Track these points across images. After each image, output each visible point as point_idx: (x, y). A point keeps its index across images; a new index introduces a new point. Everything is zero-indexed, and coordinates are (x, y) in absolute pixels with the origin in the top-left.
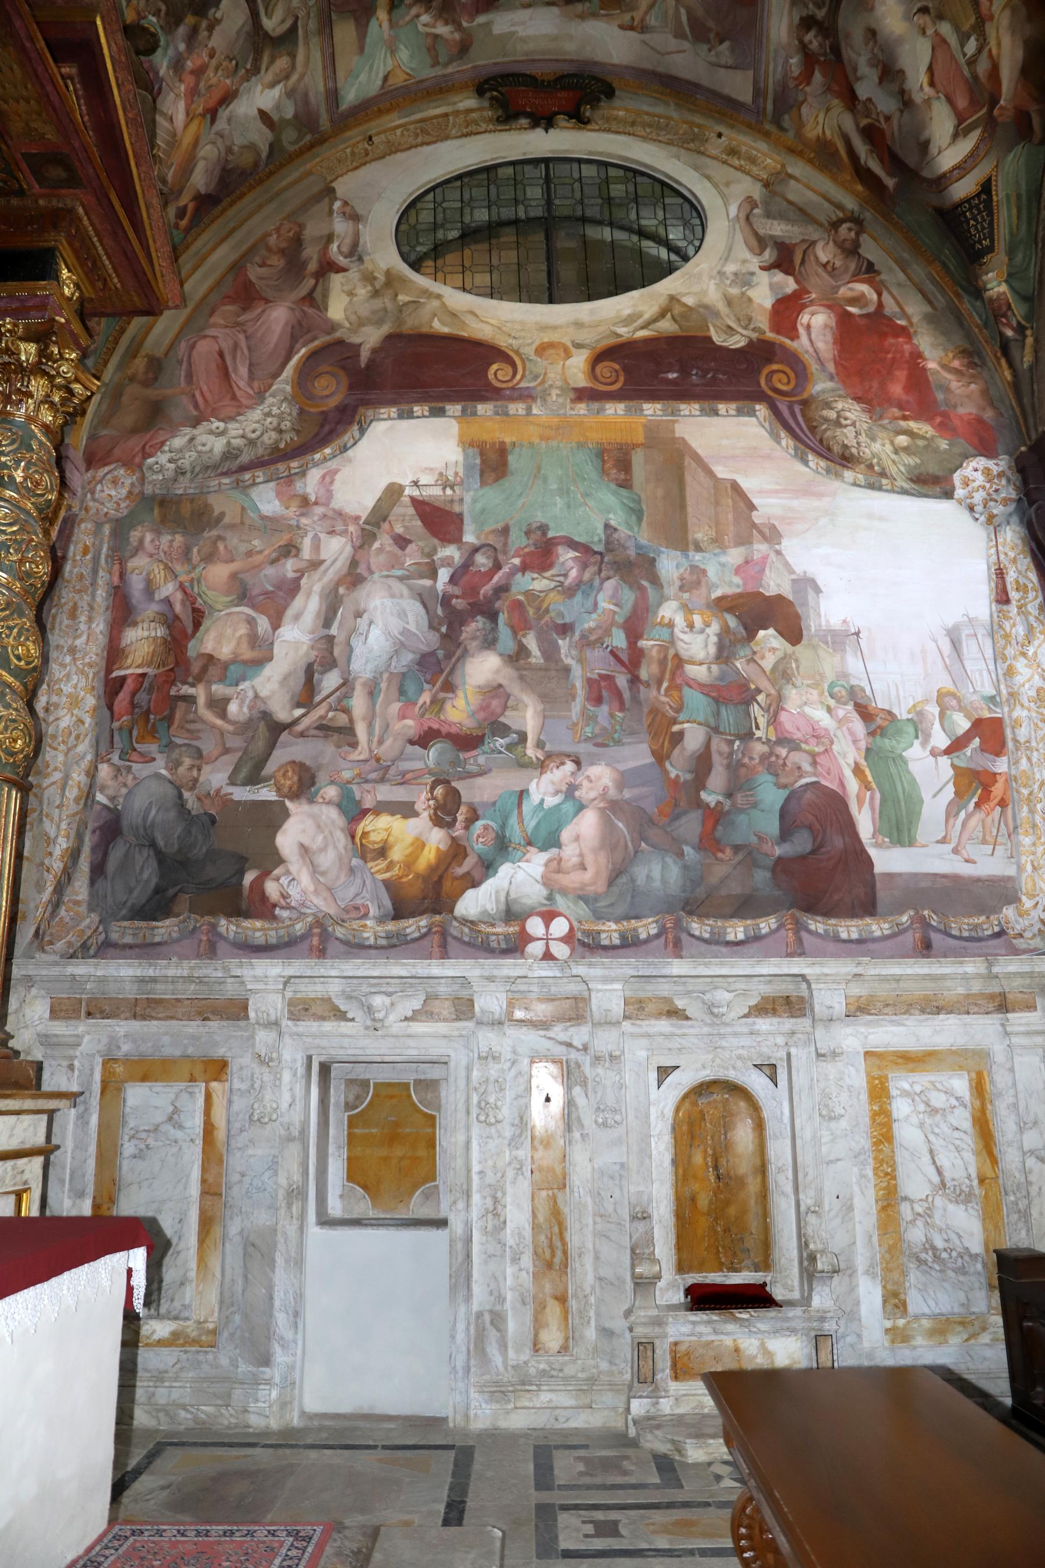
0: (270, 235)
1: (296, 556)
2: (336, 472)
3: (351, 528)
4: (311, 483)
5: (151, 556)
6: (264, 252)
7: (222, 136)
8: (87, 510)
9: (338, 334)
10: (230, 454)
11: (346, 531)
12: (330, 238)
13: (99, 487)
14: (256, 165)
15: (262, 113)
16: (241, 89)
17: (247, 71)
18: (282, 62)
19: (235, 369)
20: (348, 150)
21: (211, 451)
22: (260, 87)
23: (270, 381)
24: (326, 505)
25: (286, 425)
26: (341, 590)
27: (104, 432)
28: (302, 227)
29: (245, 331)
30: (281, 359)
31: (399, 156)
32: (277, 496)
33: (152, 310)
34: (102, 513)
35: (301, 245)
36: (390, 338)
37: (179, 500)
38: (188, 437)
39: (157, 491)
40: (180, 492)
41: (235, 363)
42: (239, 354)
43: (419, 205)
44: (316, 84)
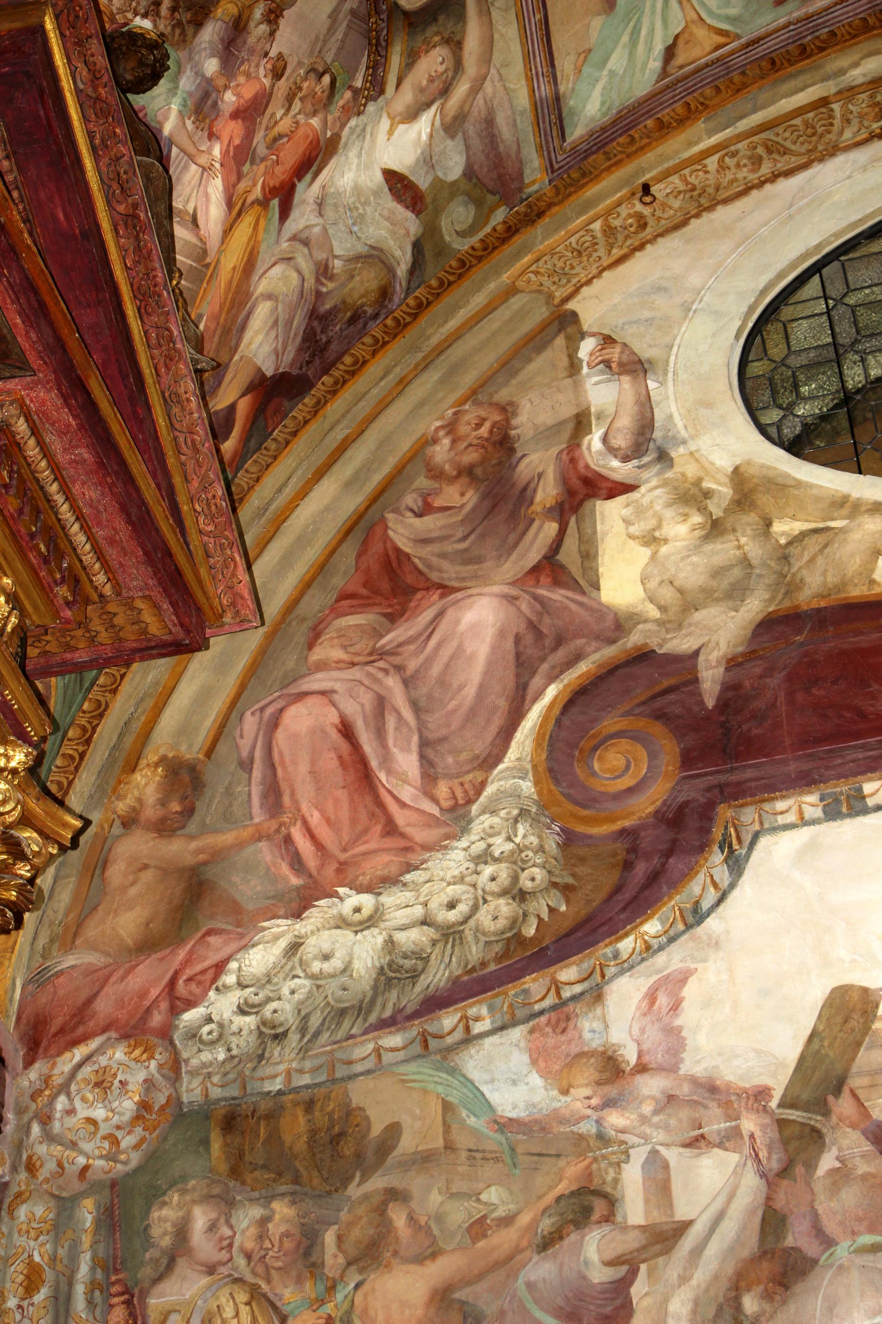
0: (435, 441)
1: (608, 1218)
2: (682, 978)
3: (749, 1124)
4: (620, 1018)
5: (211, 1269)
6: (423, 482)
7: (306, 243)
8: (31, 1168)
9: (634, 639)
10: (395, 971)
11: (737, 1132)
12: (581, 423)
13: (61, 1103)
14: (385, 293)
15: (393, 178)
17: (356, 92)
18: (433, 62)
19: (386, 759)
20: (597, 226)
21: (346, 969)
22: (385, 123)
23: (479, 776)
24: (671, 1069)
25: (534, 876)
26: (750, 1304)
27: (70, 961)
28: (508, 410)
29: (399, 668)
30: (497, 722)
31: (722, 214)
32: (534, 1062)
33: (185, 644)
34: (71, 1171)
35: (512, 450)
36: (768, 625)
37: (273, 1111)
38: (283, 943)
39: (216, 1093)
40: (277, 1085)
41: (384, 745)
42: (391, 722)
43: (787, 312)
44: (510, 91)
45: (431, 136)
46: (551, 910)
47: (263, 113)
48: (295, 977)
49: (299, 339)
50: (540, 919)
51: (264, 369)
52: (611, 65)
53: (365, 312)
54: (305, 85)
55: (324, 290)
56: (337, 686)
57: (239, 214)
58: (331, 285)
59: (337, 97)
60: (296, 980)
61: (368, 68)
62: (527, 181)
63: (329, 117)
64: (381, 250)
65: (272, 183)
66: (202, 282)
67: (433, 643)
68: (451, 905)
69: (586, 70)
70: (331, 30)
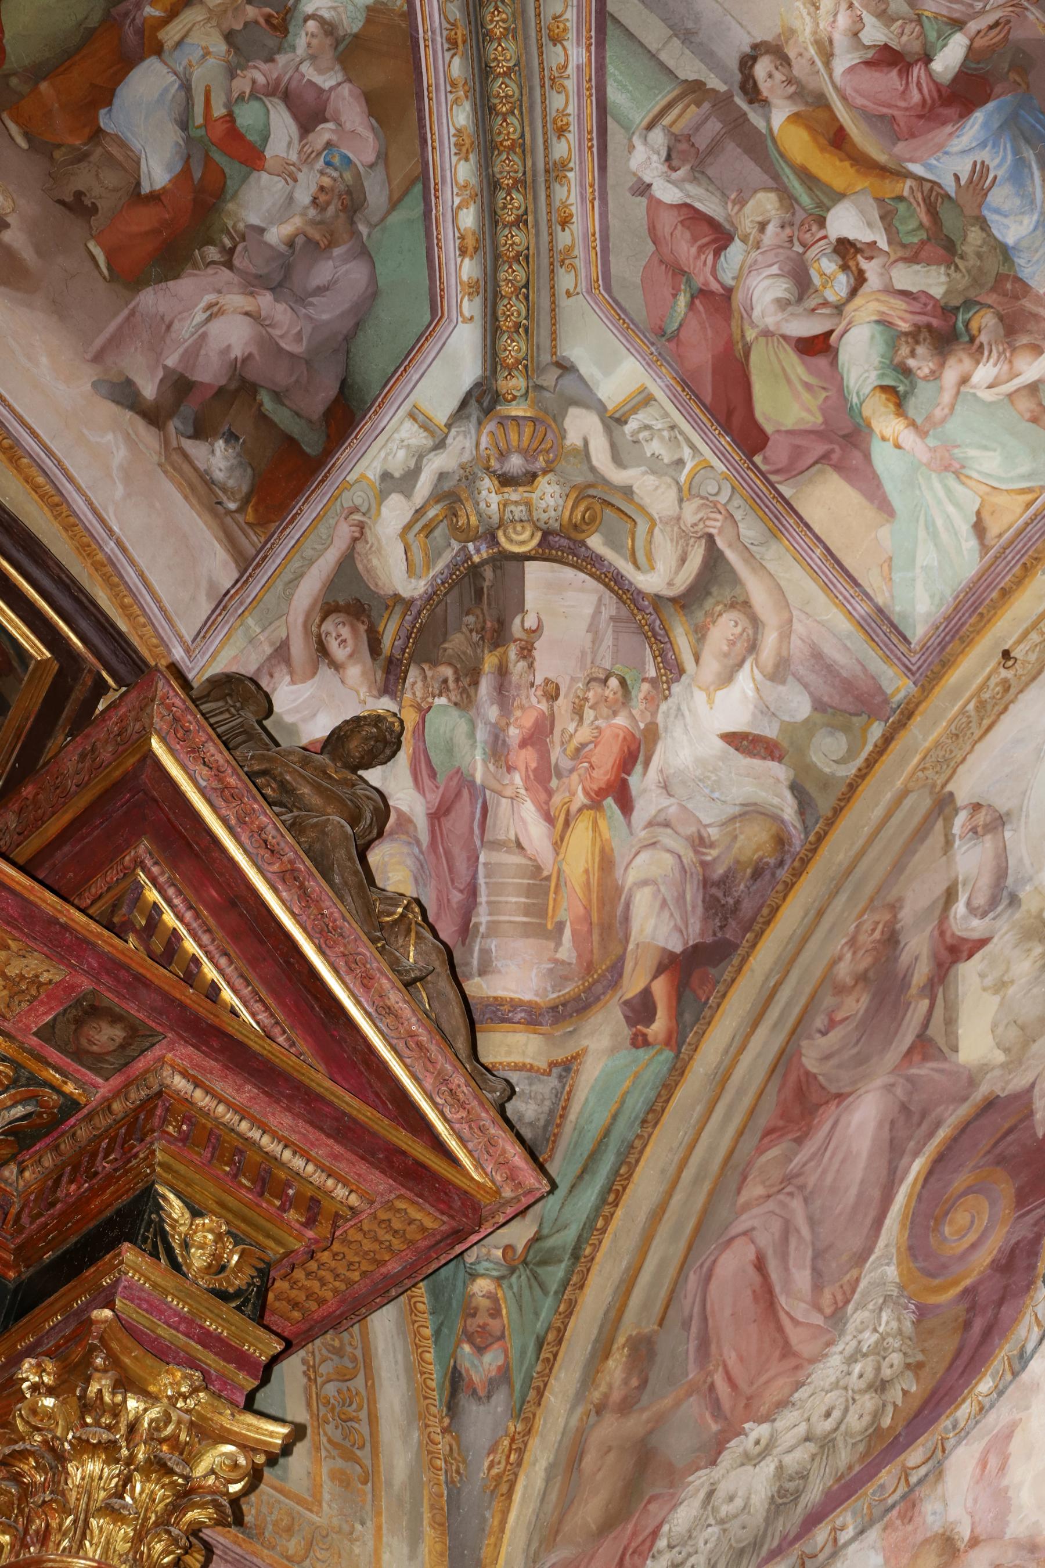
0: (840, 958)
6: (828, 1001)
7: (667, 825)
9: (983, 1090)
14: (781, 841)
15: (736, 740)
16: (660, 719)
17: (653, 682)
18: (726, 628)
22: (700, 697)
30: (872, 1213)
41: (786, 1269)
44: (826, 623)
45: (757, 689)
46: (905, 1393)
47: (552, 732)
48: (710, 1525)
49: (700, 910)
50: (895, 1405)
51: (670, 948)
52: (919, 562)
53: (767, 864)
54: (590, 695)
55: (709, 858)
56: (755, 1223)
57: (567, 824)
58: (714, 853)
59: (633, 693)
60: (710, 1530)
61: (655, 658)
62: (889, 691)
63: (634, 712)
64: (755, 804)
65: (595, 787)
66: (547, 894)
67: (828, 1154)
68: (828, 1415)
69: (896, 576)
70: (597, 640)
